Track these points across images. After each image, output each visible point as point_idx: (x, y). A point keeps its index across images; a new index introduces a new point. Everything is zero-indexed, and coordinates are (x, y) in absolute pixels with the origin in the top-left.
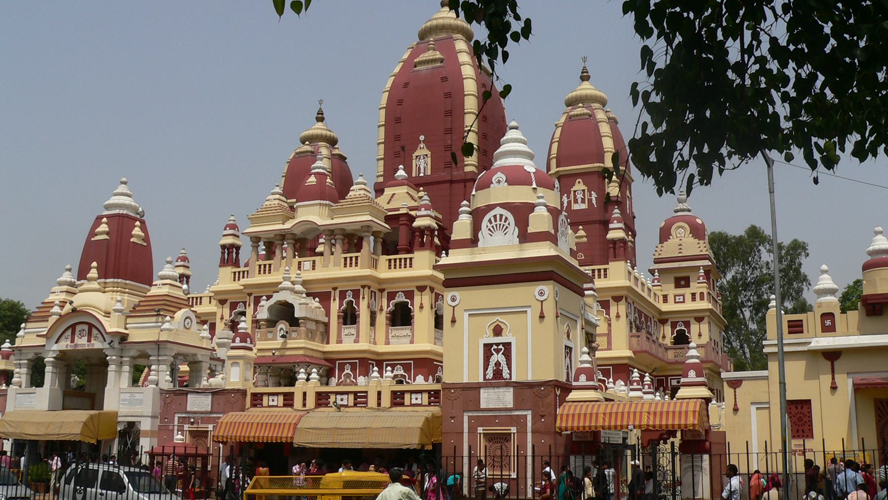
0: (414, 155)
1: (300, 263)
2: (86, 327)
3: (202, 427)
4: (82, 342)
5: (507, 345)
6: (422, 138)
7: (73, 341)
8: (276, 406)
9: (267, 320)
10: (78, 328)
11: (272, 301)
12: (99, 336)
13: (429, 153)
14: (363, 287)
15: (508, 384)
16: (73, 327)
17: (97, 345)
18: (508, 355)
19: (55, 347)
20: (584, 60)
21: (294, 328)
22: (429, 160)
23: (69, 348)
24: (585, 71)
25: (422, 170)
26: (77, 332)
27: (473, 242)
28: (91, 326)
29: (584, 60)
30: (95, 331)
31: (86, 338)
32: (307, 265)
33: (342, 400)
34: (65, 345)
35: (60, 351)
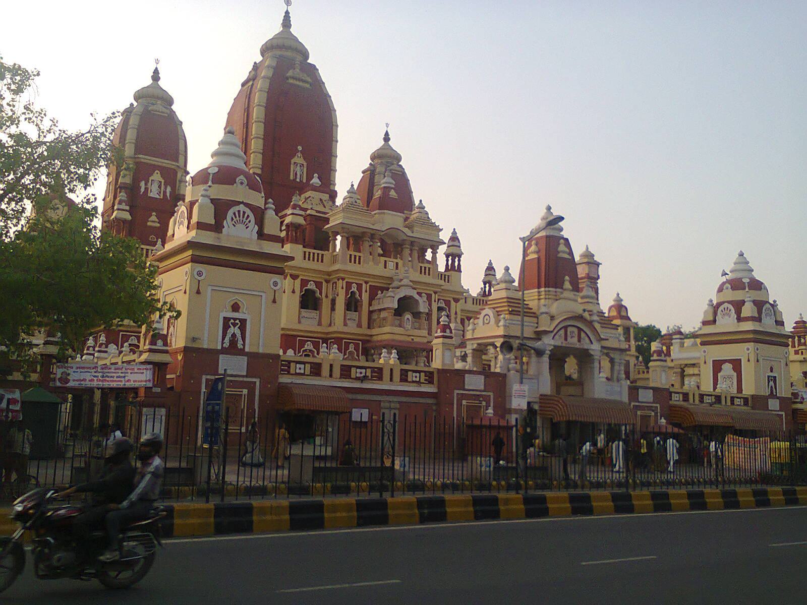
0: (293, 161)
1: (385, 261)
2: (576, 330)
3: (647, 412)
4: (573, 341)
5: (775, 377)
6: (300, 148)
7: (566, 339)
8: (303, 374)
9: (395, 310)
10: (569, 329)
11: (402, 293)
12: (587, 338)
13: (305, 164)
14: (435, 293)
15: (778, 398)
16: (566, 328)
17: (586, 344)
18: (243, 329)
19: (552, 342)
20: (387, 125)
21: (418, 320)
22: (305, 170)
23: (564, 345)
24: (387, 134)
25: (298, 176)
26: (569, 333)
27: (759, 319)
28: (580, 330)
29: (387, 125)
30: (583, 335)
31: (575, 340)
32: (391, 265)
33: (300, 369)
34: (559, 341)
35: (555, 346)
